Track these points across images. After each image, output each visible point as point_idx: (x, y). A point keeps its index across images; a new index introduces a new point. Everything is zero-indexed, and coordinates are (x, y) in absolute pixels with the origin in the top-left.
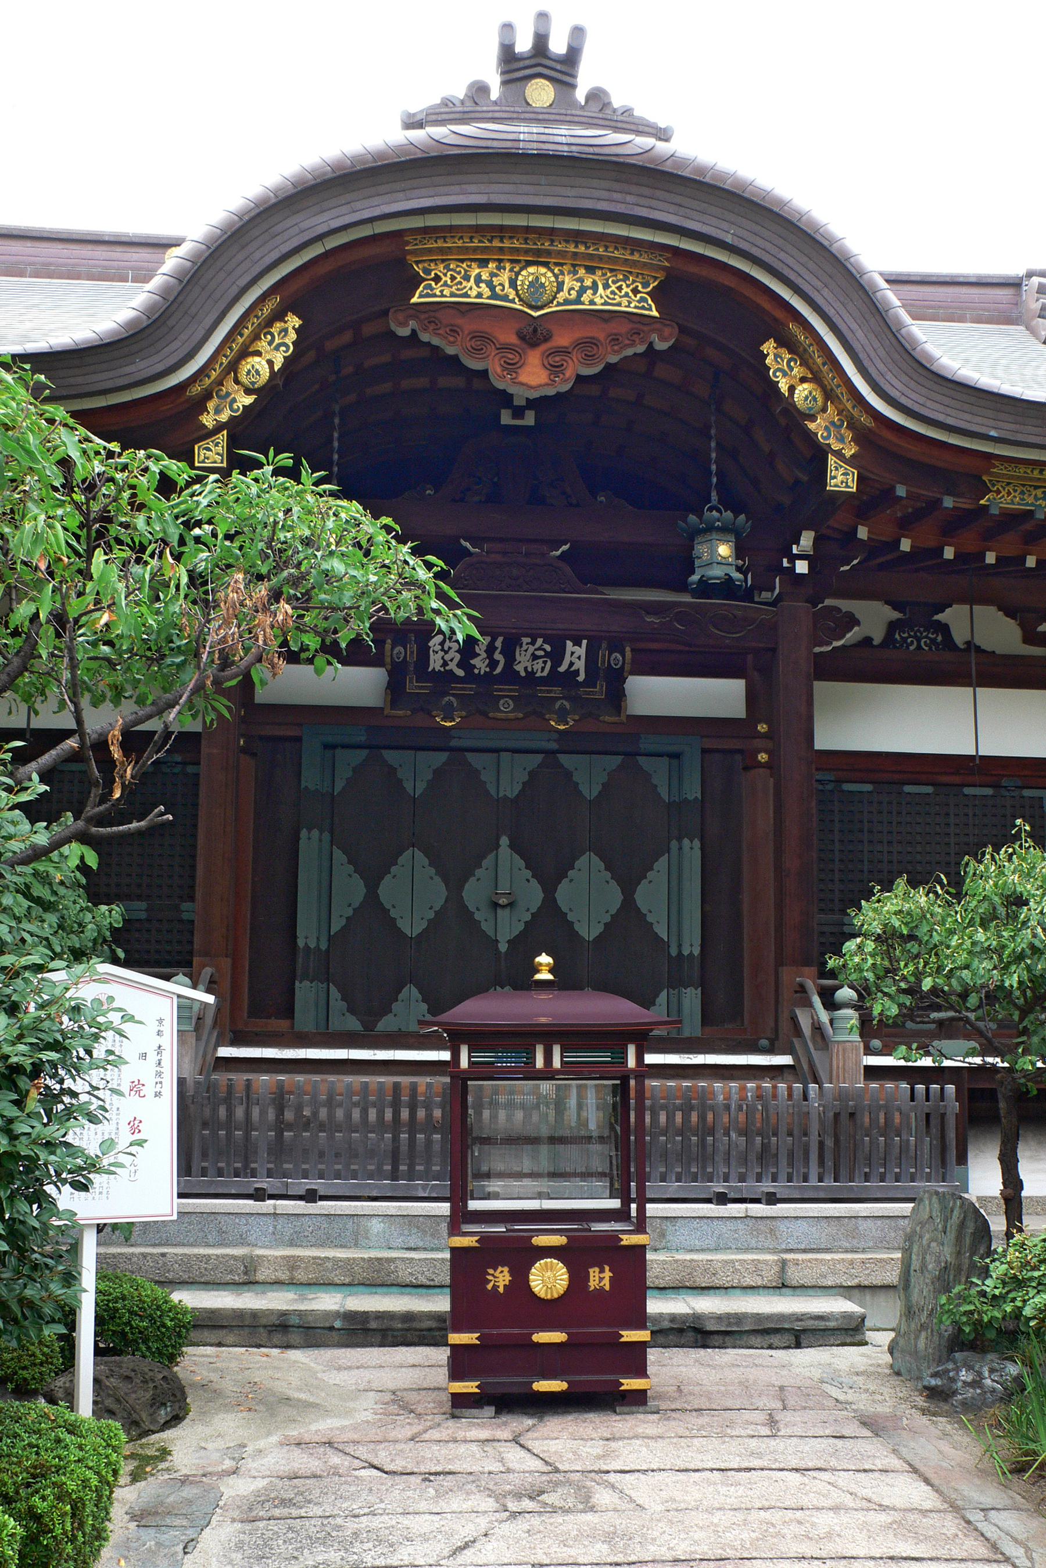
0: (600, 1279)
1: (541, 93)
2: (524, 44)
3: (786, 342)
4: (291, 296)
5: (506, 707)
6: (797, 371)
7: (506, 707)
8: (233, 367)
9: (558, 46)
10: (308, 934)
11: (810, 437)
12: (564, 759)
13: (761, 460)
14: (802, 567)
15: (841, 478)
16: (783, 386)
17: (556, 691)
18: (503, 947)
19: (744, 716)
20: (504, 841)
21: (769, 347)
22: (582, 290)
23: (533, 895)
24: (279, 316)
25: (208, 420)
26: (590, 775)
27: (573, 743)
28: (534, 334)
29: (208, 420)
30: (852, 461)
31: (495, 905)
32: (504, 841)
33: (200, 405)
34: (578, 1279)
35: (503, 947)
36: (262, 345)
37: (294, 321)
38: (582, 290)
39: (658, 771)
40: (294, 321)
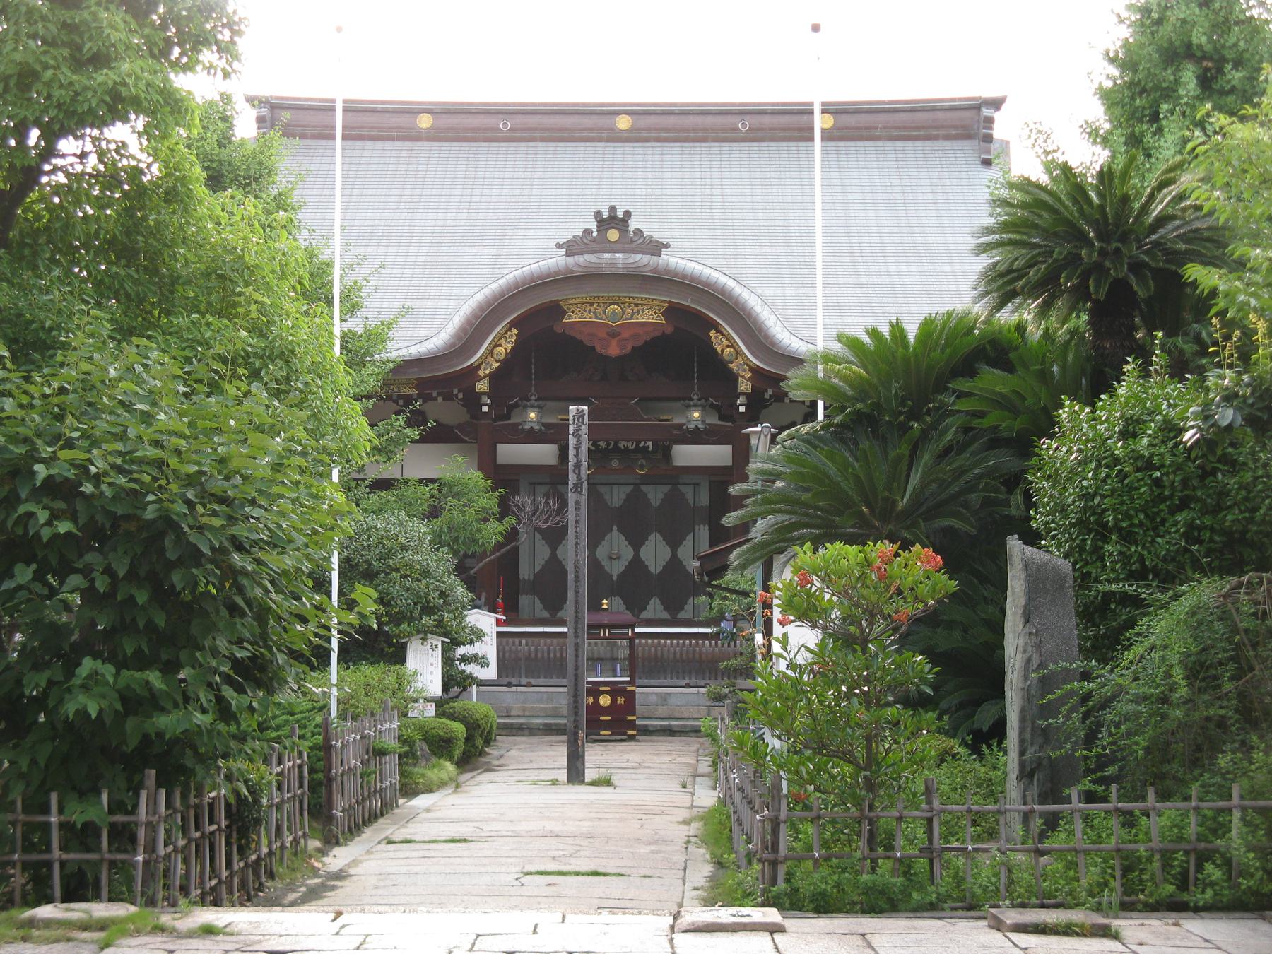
0: (621, 700)
1: (613, 235)
2: (605, 215)
3: (718, 331)
4: (513, 324)
5: (615, 464)
6: (725, 342)
7: (615, 464)
8: (492, 352)
9: (620, 214)
10: (525, 572)
11: (730, 371)
12: (644, 488)
13: (717, 375)
14: (742, 409)
15: (745, 386)
16: (719, 350)
17: (639, 456)
18: (615, 578)
19: (730, 463)
20: (615, 528)
21: (712, 333)
22: (633, 314)
23: (628, 553)
24: (509, 330)
25: (481, 373)
26: (655, 495)
27: (647, 480)
28: (613, 334)
29: (481, 373)
30: (749, 379)
31: (611, 558)
32: (615, 528)
33: (478, 368)
34: (614, 700)
35: (615, 578)
36: (503, 341)
37: (515, 331)
38: (633, 314)
39: (688, 491)
40: (515, 331)
